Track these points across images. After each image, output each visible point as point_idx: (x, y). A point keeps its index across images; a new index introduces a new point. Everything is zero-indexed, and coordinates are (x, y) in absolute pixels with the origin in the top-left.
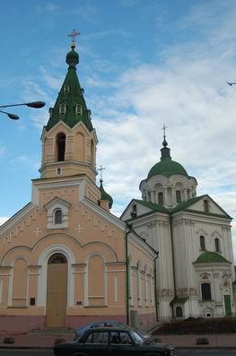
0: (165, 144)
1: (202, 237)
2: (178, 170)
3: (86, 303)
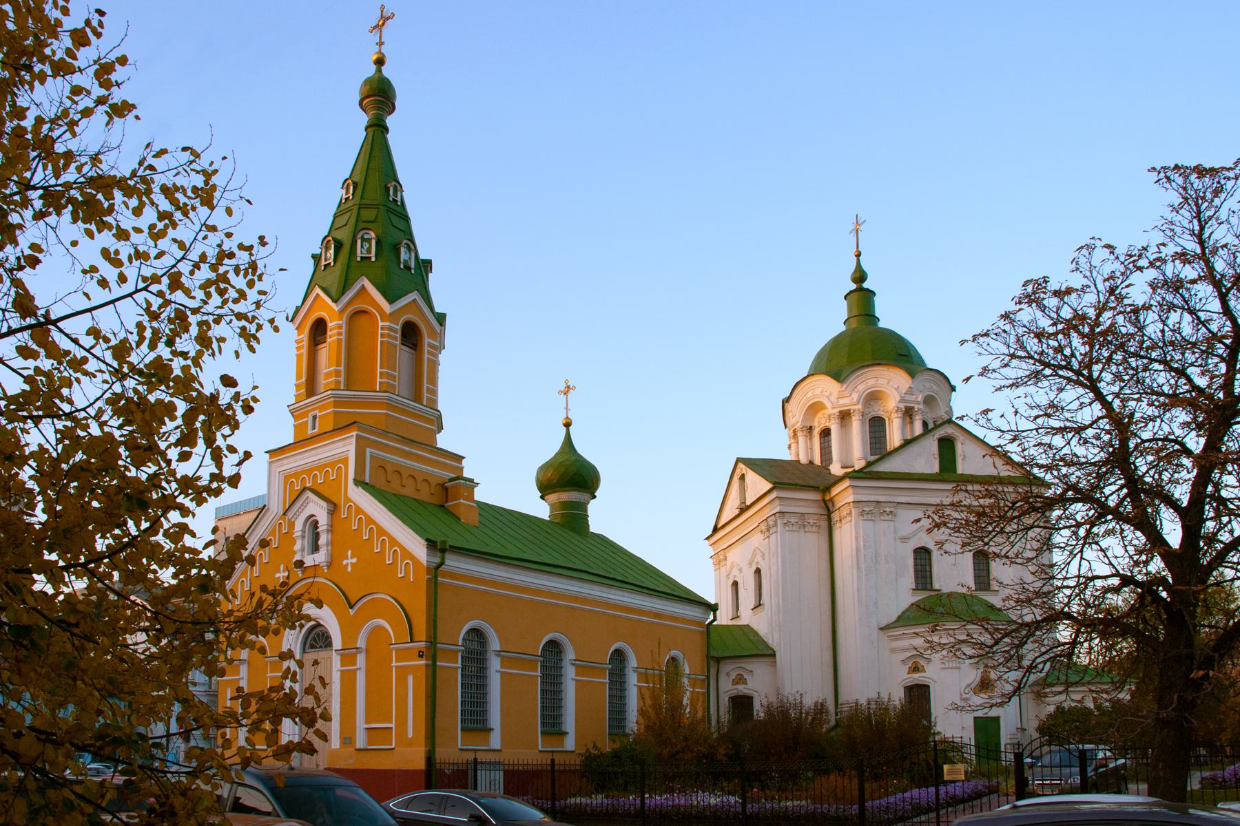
2: (899, 353)
3: (361, 742)
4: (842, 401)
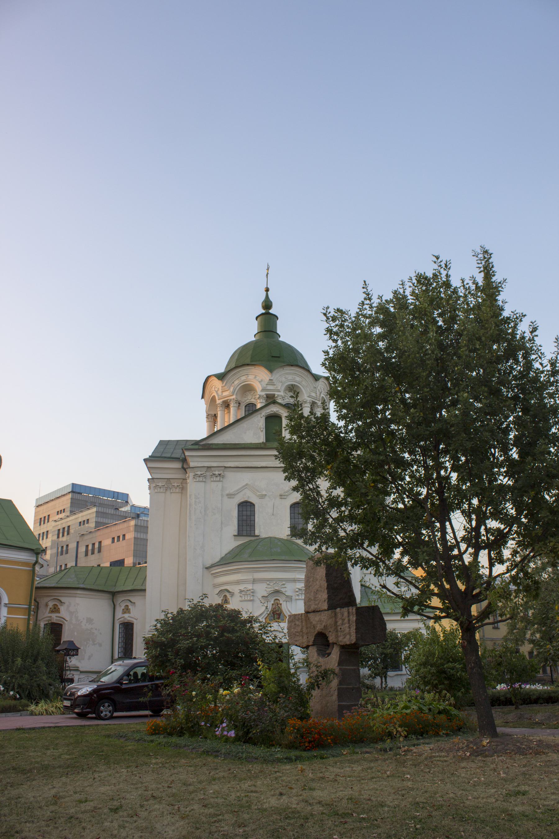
0: (267, 305)
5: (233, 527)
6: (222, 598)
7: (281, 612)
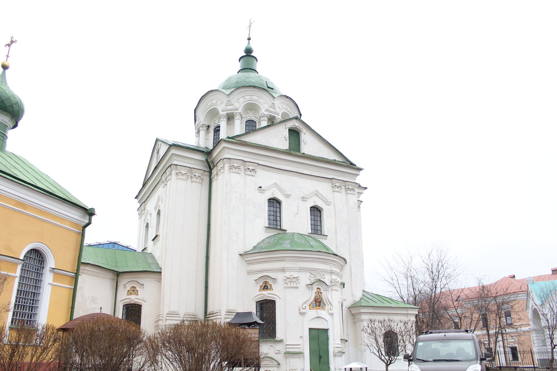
0: (248, 52)
1: (274, 203)
4: (229, 107)
5: (263, 220)
6: (261, 284)
7: (322, 300)
